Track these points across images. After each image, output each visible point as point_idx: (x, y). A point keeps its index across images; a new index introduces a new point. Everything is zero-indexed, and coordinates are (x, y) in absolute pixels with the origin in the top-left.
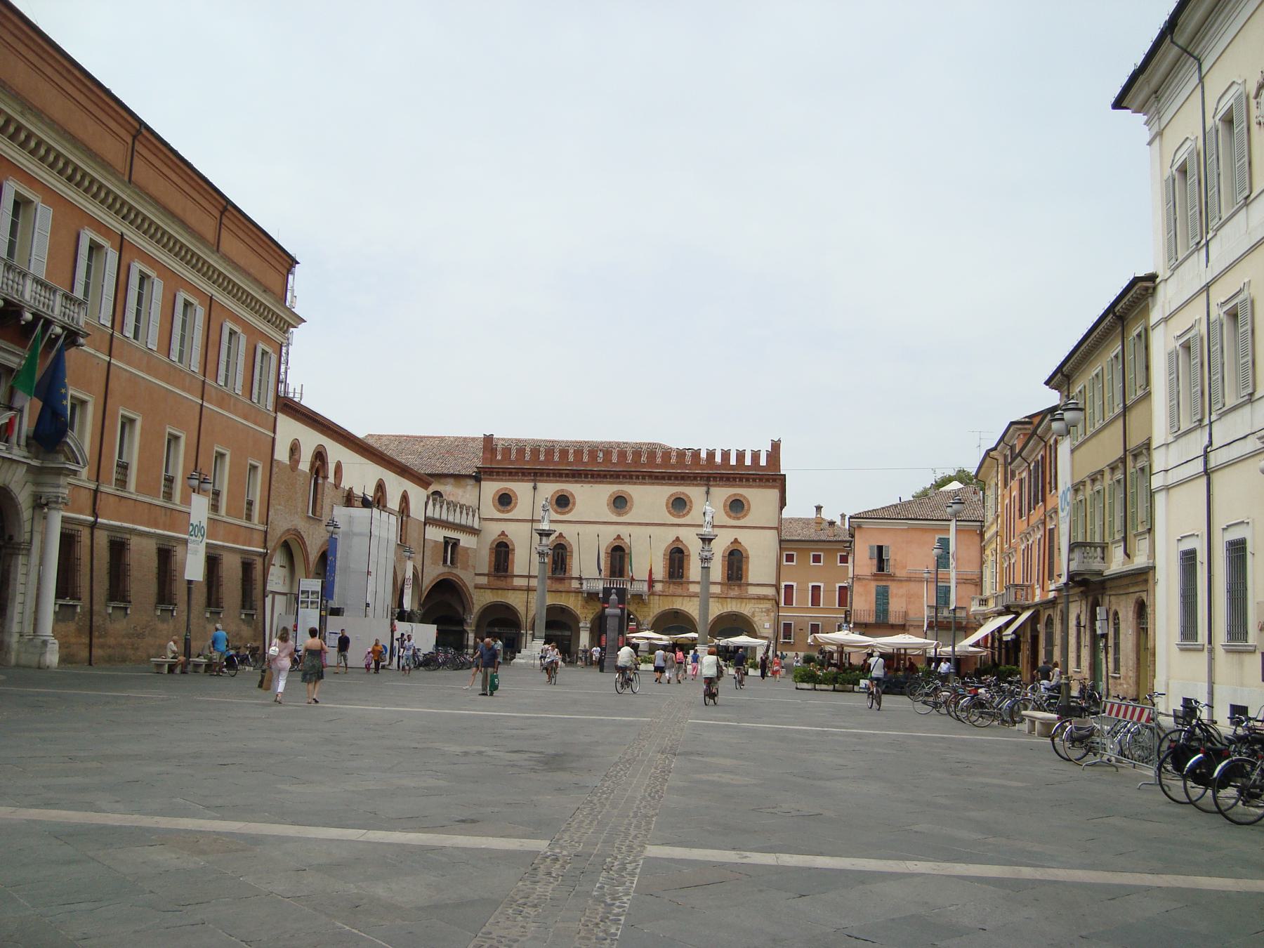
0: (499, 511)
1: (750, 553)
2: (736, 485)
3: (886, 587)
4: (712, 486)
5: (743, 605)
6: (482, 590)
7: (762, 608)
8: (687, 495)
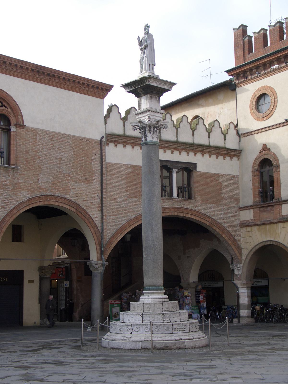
0: (259, 119)
6: (249, 229)
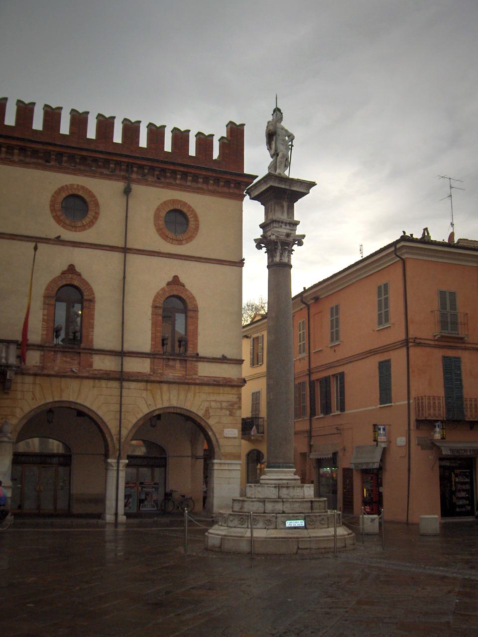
1: (201, 304)
2: (177, 185)
3: (458, 360)
4: (135, 181)
5: (190, 395)
7: (221, 402)
8: (89, 193)
